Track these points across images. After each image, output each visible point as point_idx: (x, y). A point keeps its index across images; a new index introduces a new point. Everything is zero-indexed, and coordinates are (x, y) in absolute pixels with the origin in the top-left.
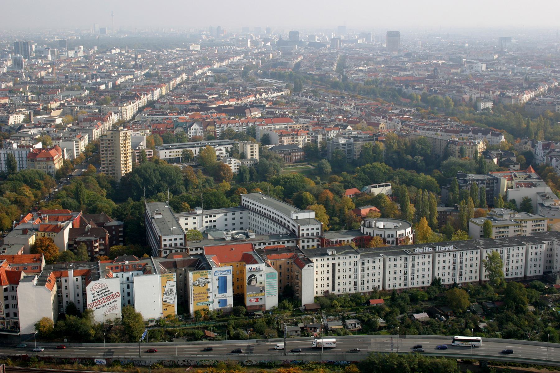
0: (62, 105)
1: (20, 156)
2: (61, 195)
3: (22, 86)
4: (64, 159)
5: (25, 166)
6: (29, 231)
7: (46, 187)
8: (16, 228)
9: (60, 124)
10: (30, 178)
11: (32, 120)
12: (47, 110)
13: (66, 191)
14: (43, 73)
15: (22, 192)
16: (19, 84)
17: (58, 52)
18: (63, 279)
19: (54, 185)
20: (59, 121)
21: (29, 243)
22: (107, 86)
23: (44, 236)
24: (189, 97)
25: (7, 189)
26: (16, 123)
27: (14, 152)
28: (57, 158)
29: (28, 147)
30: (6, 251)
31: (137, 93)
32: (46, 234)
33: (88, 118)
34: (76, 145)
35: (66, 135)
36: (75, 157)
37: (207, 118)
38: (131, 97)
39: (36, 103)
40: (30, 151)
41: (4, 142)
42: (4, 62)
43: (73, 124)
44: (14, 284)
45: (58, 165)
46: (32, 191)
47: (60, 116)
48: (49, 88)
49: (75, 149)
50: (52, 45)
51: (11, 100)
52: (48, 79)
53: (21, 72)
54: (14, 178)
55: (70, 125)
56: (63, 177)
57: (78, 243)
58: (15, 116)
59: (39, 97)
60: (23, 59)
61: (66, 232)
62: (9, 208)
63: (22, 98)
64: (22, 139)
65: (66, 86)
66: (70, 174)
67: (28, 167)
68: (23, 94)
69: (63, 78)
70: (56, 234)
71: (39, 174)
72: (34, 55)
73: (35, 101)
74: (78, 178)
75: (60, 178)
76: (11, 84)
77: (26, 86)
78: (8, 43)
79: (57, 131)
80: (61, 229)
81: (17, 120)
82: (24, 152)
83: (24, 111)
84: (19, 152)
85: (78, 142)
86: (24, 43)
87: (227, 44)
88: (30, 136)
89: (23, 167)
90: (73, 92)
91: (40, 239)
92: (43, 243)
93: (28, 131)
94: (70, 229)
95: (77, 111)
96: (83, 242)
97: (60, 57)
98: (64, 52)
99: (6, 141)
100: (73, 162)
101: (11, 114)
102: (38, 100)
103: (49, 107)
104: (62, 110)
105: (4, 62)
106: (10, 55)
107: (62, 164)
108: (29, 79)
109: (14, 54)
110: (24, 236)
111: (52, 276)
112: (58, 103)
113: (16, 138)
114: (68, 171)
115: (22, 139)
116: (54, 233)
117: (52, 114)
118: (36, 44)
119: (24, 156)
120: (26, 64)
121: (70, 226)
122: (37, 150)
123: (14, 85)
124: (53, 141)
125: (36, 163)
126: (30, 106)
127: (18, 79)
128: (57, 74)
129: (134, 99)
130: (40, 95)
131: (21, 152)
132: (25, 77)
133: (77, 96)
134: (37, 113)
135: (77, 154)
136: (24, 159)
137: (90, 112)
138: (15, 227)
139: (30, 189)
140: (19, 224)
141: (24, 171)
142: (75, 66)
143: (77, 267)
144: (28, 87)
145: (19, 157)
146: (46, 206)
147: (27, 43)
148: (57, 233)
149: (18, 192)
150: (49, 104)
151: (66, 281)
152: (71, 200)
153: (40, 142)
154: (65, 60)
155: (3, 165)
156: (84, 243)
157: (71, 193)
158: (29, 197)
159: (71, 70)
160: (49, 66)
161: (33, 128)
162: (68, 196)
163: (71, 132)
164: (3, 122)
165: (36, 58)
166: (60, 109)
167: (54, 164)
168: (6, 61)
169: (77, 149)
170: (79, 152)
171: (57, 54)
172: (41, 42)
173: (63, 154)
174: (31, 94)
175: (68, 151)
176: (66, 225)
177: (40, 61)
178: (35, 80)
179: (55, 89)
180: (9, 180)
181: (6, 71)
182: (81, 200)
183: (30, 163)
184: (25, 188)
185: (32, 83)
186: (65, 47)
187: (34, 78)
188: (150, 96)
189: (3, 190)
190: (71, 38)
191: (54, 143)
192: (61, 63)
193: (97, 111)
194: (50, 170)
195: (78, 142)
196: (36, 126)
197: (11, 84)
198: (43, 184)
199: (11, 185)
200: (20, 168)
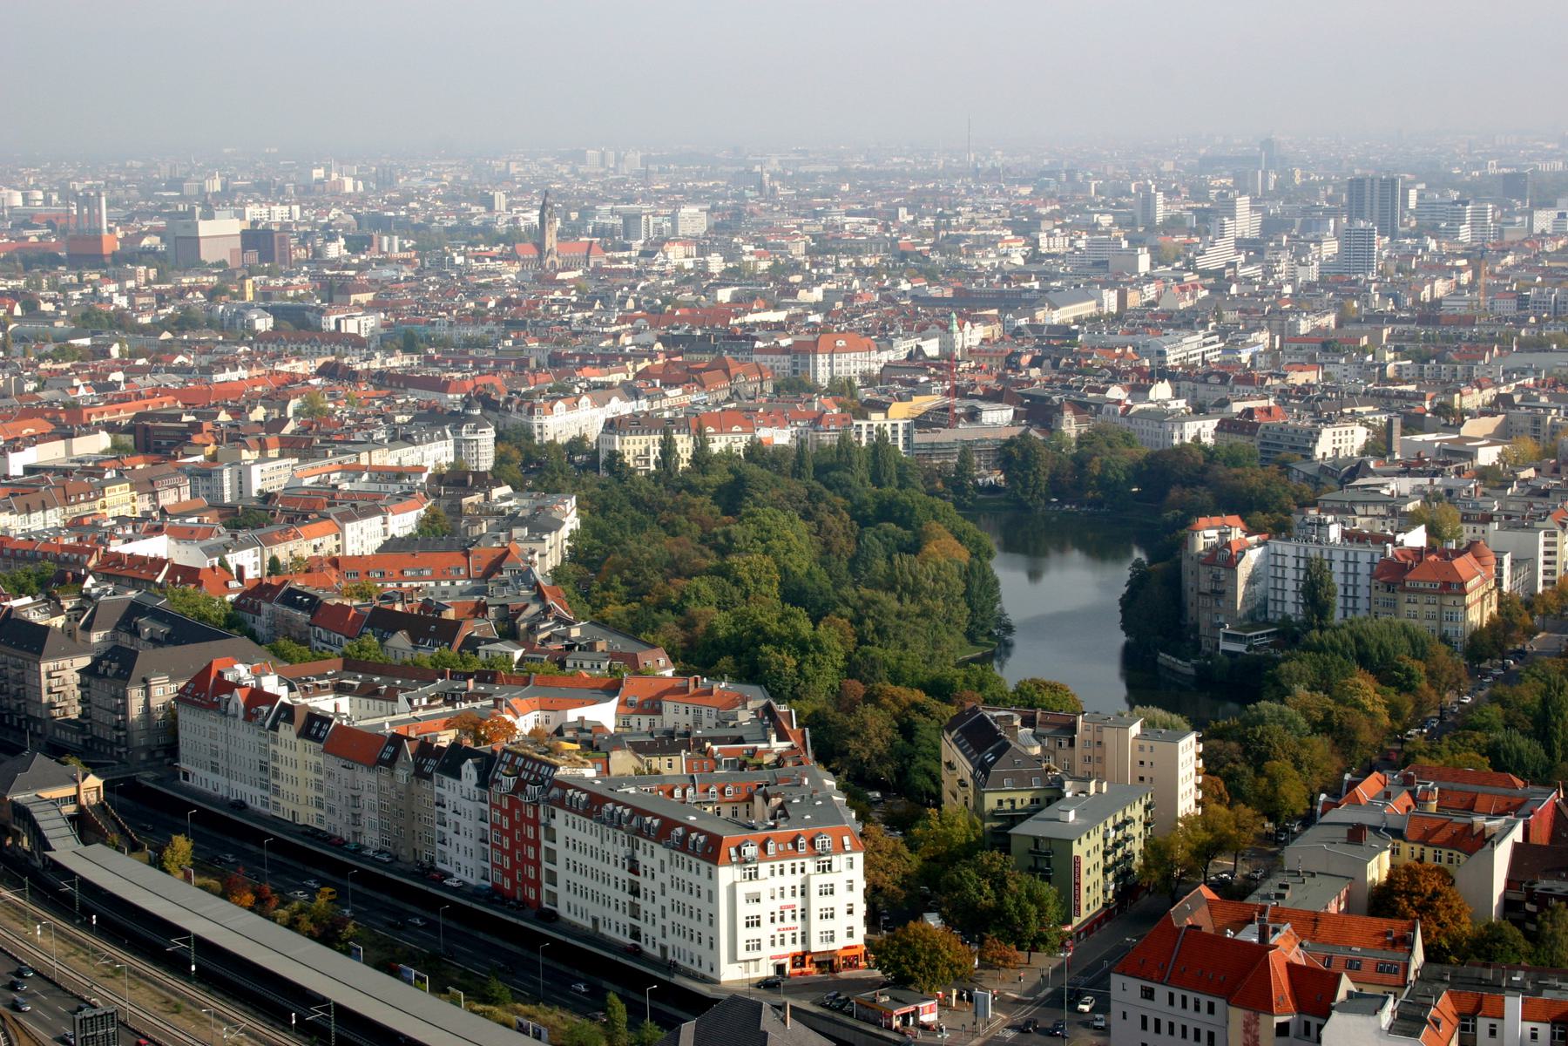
0: (1503, 401)
1: (1351, 568)
2: (1484, 720)
3: (1367, 327)
4: (1500, 594)
5: (1362, 604)
6: (1369, 834)
7: (1431, 686)
8: (1326, 819)
9: (1493, 467)
10: (1380, 646)
11: (1396, 447)
12: (1450, 417)
13: (1503, 707)
14: (1441, 287)
15: (1350, 692)
16: (1358, 321)
17: (1498, 214)
18: (1483, 1024)
19: (1459, 680)
20: (1488, 456)
21: (1369, 878)
23: (1421, 860)
25: (1300, 680)
26: (1341, 455)
27: (1330, 553)
28: (1476, 587)
29: (1380, 540)
30: (1288, 894)
32: (1429, 852)
34: (1546, 544)
35: (1512, 507)
36: (1540, 589)
39: (1412, 388)
40: (1385, 554)
41: (1297, 518)
42: (1312, 245)
43: (1538, 470)
44: (1314, 1015)
45: (1479, 611)
46: (1383, 695)
47: (1494, 439)
48: (1459, 337)
49: (1541, 558)
50: (1475, 191)
51: (1327, 376)
52: (1460, 307)
53: (1368, 281)
54: (1327, 643)
55: (1529, 473)
56: (1492, 657)
57: (1542, 900)
58: (1337, 430)
59: (1422, 369)
60: (1377, 237)
61: (1502, 856)
62: (1303, 745)
63: (1365, 371)
64: (1359, 510)
65: (1519, 336)
66: (1519, 646)
67: (1374, 608)
68: (1369, 358)
69: (1508, 307)
70: (1462, 856)
71: (1410, 638)
72: (1413, 224)
73: (1407, 383)
74: (1548, 664)
75: (1481, 659)
76: (1330, 320)
77: (1381, 331)
78: (1327, 182)
79: (1481, 490)
80: (1485, 841)
81: (1343, 445)
82: (1364, 558)
83: (1369, 413)
84: (1347, 554)
85: (1554, 535)
86: (1384, 184)
87: (935, 176)
88: (1384, 502)
89: (1355, 610)
90: (1543, 354)
91: (1408, 868)
92: (1416, 882)
93: (1382, 485)
94: (1516, 846)
95: (1554, 426)
96: (1560, 898)
97: (1501, 231)
98: (1517, 214)
99: (1305, 515)
100: (1531, 602)
101: (1326, 423)
102: (1419, 378)
103: (1457, 407)
104: (1500, 418)
105: (1312, 245)
106: (1332, 222)
107: (1494, 609)
108: (1390, 306)
109: (1345, 220)
110: (1353, 851)
111: (1443, 1006)
112: (1489, 394)
113: (1337, 505)
114: (1513, 635)
115: (1359, 510)
116: (1456, 853)
117: (1464, 431)
118: (1423, 186)
119: (1364, 569)
120: (1385, 254)
121: (1517, 835)
122: (1410, 554)
123: (1339, 324)
124: (1465, 526)
125: (1405, 597)
126: (1389, 397)
127: (1355, 304)
128: (1489, 290)
130: (1427, 361)
131: (1356, 555)
132: (1377, 297)
133: (1556, 371)
134: (1414, 424)
135: (1549, 578)
136: (1363, 580)
138: (1322, 815)
139: (1378, 685)
140: (1338, 806)
141: (1360, 622)
142: (1552, 264)
143: (1539, 990)
144: (1386, 332)
145: (1346, 574)
146: (1432, 753)
147: (1393, 182)
148: (1470, 853)
149: (1336, 693)
150: (1457, 396)
151: (1493, 1033)
152: (1523, 743)
153: (1419, 525)
154: (1521, 243)
155: (1290, 597)
156: (1563, 904)
157: (1522, 716)
158: (1372, 715)
159: (1539, 279)
160: (1463, 262)
161: (1400, 474)
162: (1509, 724)
163: (1531, 500)
164: (1296, 448)
165: (1418, 234)
166: (1493, 415)
167: (1466, 608)
168: (1318, 242)
169: (1549, 558)
170: (1553, 572)
171: (1494, 220)
172: (1436, 179)
173: (1500, 573)
174: (1396, 359)
175: (1515, 563)
176: (1501, 829)
177: (1432, 245)
178: (1410, 310)
179: (1478, 346)
180: (1308, 647)
181: (1314, 277)
182: (1557, 744)
183: (1383, 595)
184: (1362, 683)
185: (1402, 321)
186: (1522, 198)
187: (1409, 301)
189: (1285, 682)
190: (1544, 167)
191: (1468, 533)
192: (1504, 252)
194: (1448, 627)
195: (1554, 535)
196: (1407, 471)
197: (1330, 320)
198: (1422, 674)
199: (1315, 664)
200: (1345, 609)
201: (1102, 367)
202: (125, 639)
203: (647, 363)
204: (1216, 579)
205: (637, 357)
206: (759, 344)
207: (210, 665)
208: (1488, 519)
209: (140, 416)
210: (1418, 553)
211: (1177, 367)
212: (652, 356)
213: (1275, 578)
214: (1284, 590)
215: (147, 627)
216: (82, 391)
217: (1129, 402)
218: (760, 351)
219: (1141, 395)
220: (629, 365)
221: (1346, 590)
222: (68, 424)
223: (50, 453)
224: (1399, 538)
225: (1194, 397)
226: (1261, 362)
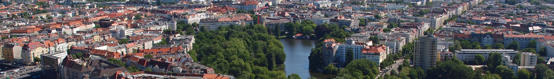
22: (422, 3)
24: (484, 15)
29: (362, 44)
31: (445, 10)
33: (406, 25)
37: (497, 31)
38: (439, 12)
73: (369, 11)
129: (442, 14)
137: (408, 21)
153: (371, 41)
188: (454, 12)
193: (413, 21)
201: (306, 8)
202: (98, 68)
203: (209, 7)
204: (329, 52)
205: (207, 6)
206: (233, 3)
207: (116, 73)
208: (384, 40)
209: (101, 20)
210: (370, 47)
211: (322, 8)
212: (210, 6)
213: (341, 52)
214: (343, 54)
215: (103, 64)
216: (89, 15)
217: (312, 15)
218: (233, 4)
219: (314, 14)
220: (206, 8)
221: (356, 54)
222: (86, 22)
223: (83, 28)
224: (367, 43)
225: (325, 14)
226: (339, 7)
